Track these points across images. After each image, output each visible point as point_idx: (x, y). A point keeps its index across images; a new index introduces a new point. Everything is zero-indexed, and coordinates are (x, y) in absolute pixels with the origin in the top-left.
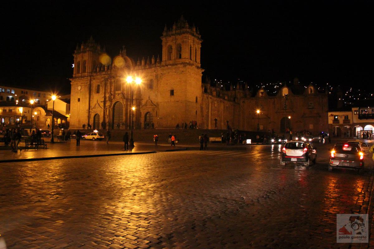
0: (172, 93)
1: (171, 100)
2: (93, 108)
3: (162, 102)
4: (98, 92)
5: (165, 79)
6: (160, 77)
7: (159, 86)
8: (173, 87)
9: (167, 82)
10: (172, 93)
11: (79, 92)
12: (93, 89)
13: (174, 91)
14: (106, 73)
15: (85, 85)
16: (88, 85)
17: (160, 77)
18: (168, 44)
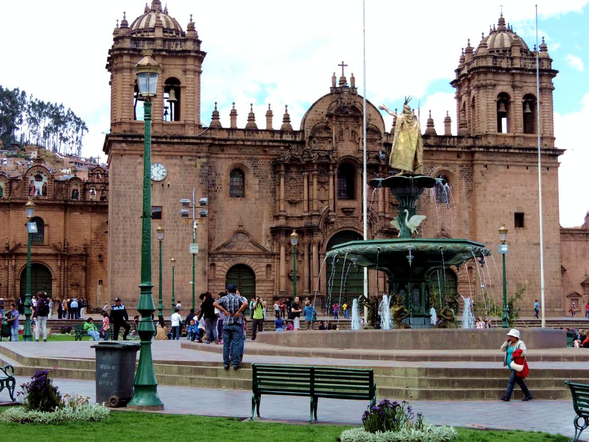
0: (519, 220)
1: (516, 240)
2: (224, 246)
3: (491, 243)
4: (238, 192)
5: (497, 181)
6: (483, 175)
7: (478, 199)
8: (524, 207)
9: (504, 190)
10: (519, 220)
11: (158, 187)
12: (217, 183)
13: (526, 217)
14: (281, 137)
15: (185, 166)
16: (199, 167)
17: (483, 175)
18: (500, 89)
